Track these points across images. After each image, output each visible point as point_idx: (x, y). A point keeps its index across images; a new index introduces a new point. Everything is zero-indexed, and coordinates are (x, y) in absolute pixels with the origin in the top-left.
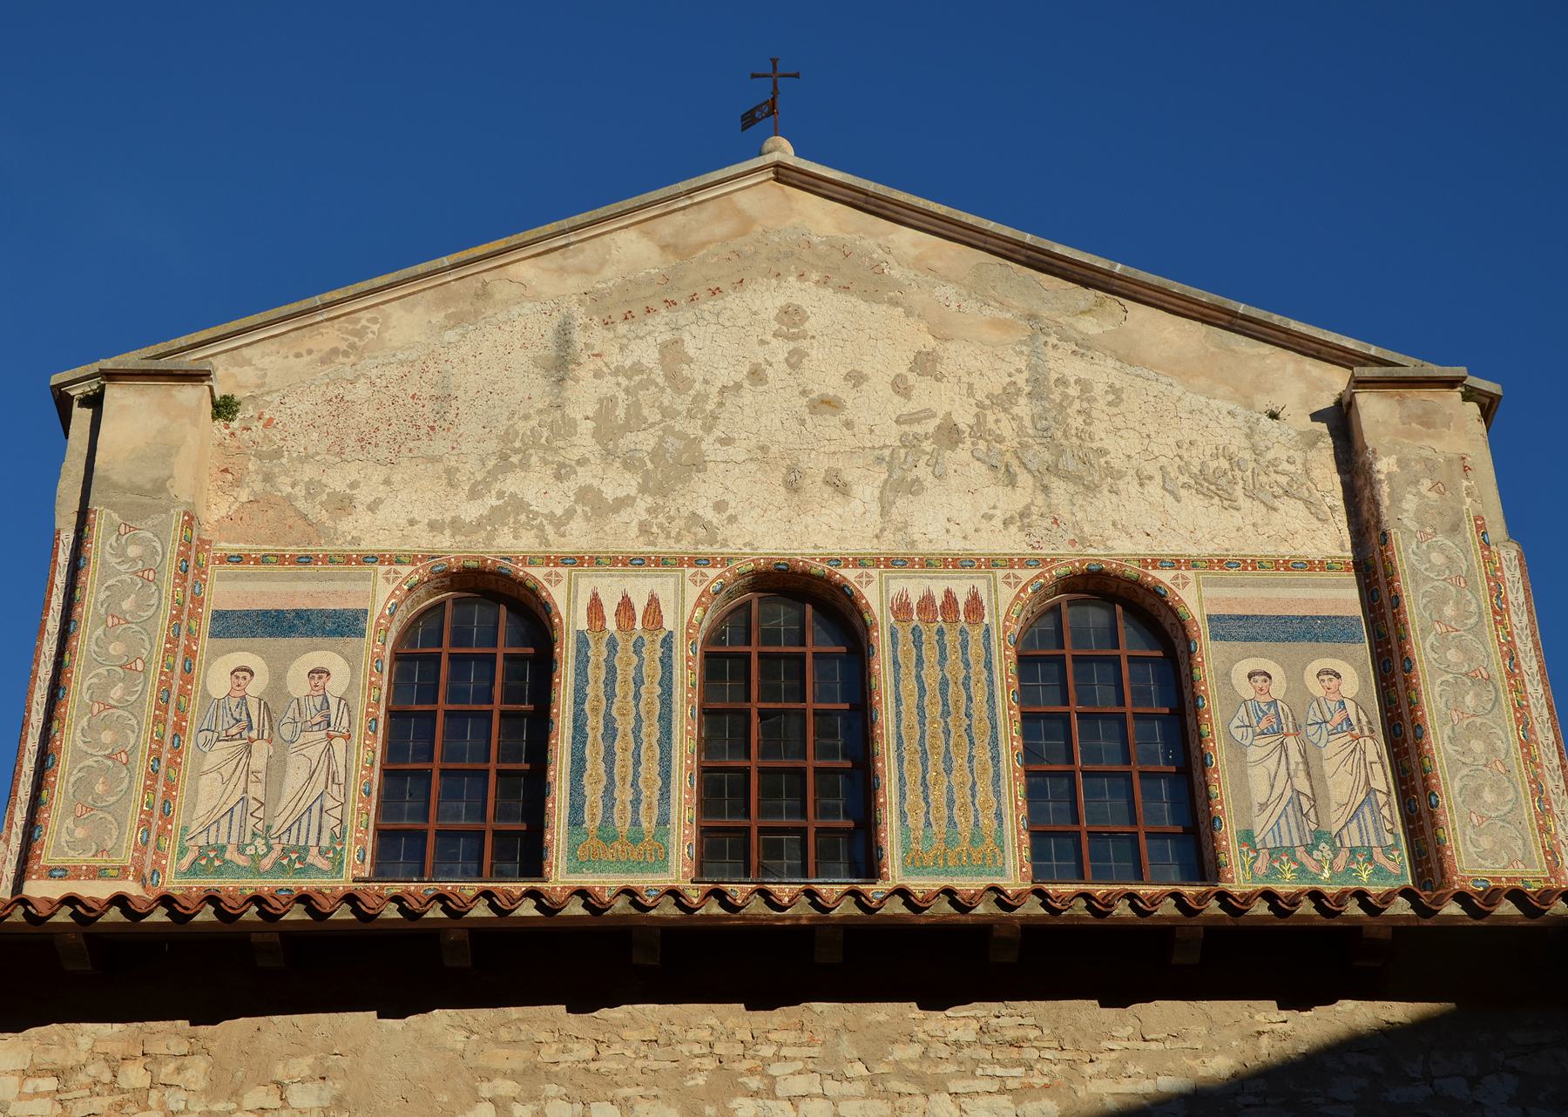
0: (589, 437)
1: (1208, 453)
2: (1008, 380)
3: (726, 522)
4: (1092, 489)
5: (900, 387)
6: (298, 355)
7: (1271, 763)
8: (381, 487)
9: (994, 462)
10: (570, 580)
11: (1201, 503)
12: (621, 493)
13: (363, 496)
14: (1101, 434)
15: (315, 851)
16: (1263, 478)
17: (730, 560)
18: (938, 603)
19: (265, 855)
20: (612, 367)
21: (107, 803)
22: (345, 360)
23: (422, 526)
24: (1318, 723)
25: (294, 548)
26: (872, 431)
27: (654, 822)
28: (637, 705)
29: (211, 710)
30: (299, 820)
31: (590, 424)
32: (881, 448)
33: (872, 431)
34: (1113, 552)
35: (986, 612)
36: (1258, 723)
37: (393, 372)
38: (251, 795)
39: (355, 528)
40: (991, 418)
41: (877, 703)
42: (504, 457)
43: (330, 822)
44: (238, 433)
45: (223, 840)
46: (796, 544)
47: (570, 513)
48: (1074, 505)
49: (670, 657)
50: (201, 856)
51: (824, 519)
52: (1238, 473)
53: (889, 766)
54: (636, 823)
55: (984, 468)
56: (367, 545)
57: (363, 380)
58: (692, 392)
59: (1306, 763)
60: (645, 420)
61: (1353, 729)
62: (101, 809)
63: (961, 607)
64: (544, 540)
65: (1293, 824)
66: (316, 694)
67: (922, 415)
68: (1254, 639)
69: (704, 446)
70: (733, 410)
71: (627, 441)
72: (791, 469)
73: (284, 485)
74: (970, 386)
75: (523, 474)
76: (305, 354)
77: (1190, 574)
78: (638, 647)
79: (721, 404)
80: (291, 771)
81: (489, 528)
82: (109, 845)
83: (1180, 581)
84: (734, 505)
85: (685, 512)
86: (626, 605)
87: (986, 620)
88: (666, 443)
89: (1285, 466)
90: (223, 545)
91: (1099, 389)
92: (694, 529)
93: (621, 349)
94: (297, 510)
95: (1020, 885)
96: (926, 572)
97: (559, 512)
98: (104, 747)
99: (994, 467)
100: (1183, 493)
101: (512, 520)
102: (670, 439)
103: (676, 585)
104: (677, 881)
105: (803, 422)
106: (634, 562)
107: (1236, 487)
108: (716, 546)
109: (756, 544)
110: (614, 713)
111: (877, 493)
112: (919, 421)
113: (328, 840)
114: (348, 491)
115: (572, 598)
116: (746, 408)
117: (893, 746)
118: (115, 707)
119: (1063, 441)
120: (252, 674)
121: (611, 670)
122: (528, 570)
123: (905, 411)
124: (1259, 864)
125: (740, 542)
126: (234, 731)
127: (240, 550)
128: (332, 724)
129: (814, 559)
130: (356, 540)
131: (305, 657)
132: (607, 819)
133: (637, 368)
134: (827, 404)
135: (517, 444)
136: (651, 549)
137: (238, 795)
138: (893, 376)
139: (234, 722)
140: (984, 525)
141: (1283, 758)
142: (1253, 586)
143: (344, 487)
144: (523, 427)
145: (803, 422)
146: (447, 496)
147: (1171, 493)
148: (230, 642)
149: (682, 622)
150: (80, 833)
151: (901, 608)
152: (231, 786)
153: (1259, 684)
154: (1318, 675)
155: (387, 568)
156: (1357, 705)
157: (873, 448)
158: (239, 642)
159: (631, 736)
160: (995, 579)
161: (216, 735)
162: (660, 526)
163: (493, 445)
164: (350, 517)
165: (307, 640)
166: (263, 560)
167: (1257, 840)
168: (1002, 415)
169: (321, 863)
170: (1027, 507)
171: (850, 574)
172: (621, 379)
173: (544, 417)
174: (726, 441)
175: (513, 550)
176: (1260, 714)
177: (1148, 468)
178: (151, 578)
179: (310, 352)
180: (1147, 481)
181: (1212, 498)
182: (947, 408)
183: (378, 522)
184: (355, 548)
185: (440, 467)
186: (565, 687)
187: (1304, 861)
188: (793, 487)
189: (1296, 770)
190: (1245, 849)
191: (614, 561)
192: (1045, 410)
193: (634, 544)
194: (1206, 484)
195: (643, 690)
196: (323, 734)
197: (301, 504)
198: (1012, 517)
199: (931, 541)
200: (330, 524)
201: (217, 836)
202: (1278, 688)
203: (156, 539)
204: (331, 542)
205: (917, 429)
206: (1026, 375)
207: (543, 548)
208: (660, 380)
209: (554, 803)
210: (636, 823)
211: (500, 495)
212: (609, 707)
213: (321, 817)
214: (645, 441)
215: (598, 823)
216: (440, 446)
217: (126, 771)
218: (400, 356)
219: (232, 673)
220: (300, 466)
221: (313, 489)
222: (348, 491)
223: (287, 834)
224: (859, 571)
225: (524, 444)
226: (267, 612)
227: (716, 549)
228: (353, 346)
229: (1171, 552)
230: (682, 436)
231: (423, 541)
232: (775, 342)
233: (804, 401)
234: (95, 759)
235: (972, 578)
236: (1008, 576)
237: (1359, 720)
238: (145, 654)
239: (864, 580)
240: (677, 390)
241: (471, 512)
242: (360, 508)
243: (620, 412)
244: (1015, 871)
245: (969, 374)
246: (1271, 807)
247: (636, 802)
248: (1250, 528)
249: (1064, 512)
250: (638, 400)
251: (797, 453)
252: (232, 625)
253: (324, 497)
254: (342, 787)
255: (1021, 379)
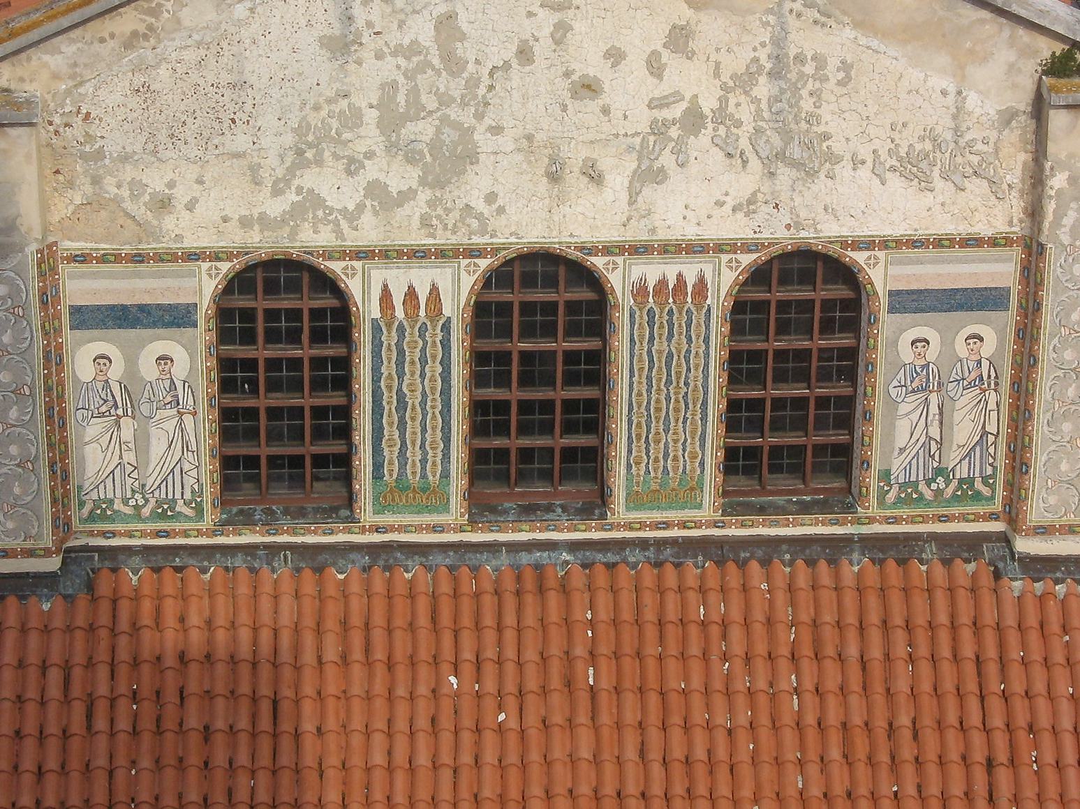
0: (373, 127)
1: (916, 135)
2: (752, 55)
3: (495, 214)
4: (812, 174)
5: (655, 67)
6: (102, 40)
7: (915, 416)
8: (196, 186)
9: (730, 150)
10: (364, 273)
11: (902, 185)
12: (405, 188)
13: (181, 195)
14: (830, 122)
15: (181, 502)
16: (959, 159)
17: (498, 250)
18: (671, 286)
19: (144, 506)
20: (392, 45)
21: (26, 502)
22: (146, 44)
23: (234, 223)
24: (957, 380)
25: (127, 247)
26: (625, 117)
27: (438, 475)
28: (422, 383)
29: (83, 391)
30: (166, 479)
31: (374, 113)
32: (633, 136)
33: (625, 117)
34: (821, 235)
35: (709, 294)
36: (912, 382)
37: (190, 56)
38: (126, 459)
39: (177, 226)
40: (732, 102)
41: (615, 374)
42: (300, 153)
43: (190, 481)
44: (61, 130)
45: (110, 495)
46: (555, 233)
47: (360, 207)
48: (794, 190)
49: (449, 340)
50: (96, 507)
51: (580, 209)
52: (938, 154)
53: (621, 428)
54: (424, 476)
55: (721, 154)
56: (191, 243)
57: (164, 66)
58: (465, 75)
59: (941, 414)
60: (424, 108)
61: (984, 384)
62: (22, 506)
63: (690, 290)
64: (339, 233)
65: (921, 464)
66: (164, 377)
67: (672, 99)
68: (922, 311)
69: (476, 137)
70: (502, 94)
71: (410, 130)
72: (553, 160)
73: (109, 184)
74: (718, 64)
75: (317, 170)
76: (108, 39)
77: (881, 254)
78: (423, 331)
79: (491, 88)
80: (154, 441)
81: (292, 223)
82: (34, 532)
83: (872, 262)
84: (501, 195)
85: (460, 204)
86: (411, 294)
87: (709, 302)
88: (443, 134)
89: (979, 147)
90: (68, 244)
91: (833, 63)
92: (468, 221)
93: (400, 27)
94: (124, 211)
95: (712, 516)
96: (665, 258)
97: (351, 207)
98: (12, 458)
99: (729, 155)
100: (889, 175)
101: (311, 216)
102: (446, 130)
103: (453, 276)
104: (456, 518)
105: (564, 108)
106: (417, 254)
107: (934, 168)
108: (487, 236)
109: (521, 234)
110: (405, 389)
111: (626, 184)
112: (667, 105)
113: (190, 494)
114: (167, 191)
115: (366, 291)
116: (514, 92)
117: (625, 411)
118: (14, 426)
119: (793, 126)
120: (110, 362)
121: (401, 353)
122: (326, 263)
123: (657, 94)
124: (890, 495)
125: (507, 232)
126: (104, 409)
127: (82, 249)
128: (181, 403)
129: (570, 247)
130: (179, 237)
131: (151, 346)
132: (402, 472)
133: (413, 49)
134: (589, 88)
135: (310, 138)
136: (432, 241)
137: (116, 460)
138: (649, 51)
139: (103, 402)
140: (717, 212)
141: (925, 410)
142: (930, 263)
143: (163, 187)
144: (314, 119)
145: (564, 108)
146: (252, 192)
147: (877, 175)
148: (87, 333)
149: (458, 308)
150: (10, 525)
151: (640, 291)
152: (109, 454)
153: (918, 350)
154: (966, 340)
155: (210, 264)
156: (990, 363)
157: (626, 135)
158: (96, 332)
159: (419, 409)
160: (720, 264)
161: (90, 412)
162: (438, 217)
163: (289, 139)
164: (171, 215)
165: (150, 332)
166: (103, 259)
167: (892, 477)
168: (742, 98)
169: (188, 511)
170: (754, 194)
171: (598, 262)
172: (401, 61)
173: (333, 107)
174: (496, 130)
175: (313, 244)
176: (915, 375)
177: (862, 151)
178: (21, 314)
179: (112, 36)
180: (859, 165)
181: (912, 180)
182: (695, 90)
183: (196, 220)
184: (179, 246)
185: (244, 162)
186: (364, 366)
187: (924, 491)
188: (554, 177)
189: (932, 421)
190: (882, 484)
191: (400, 254)
192: (782, 91)
193: (418, 238)
194: (909, 166)
195: (427, 369)
196: (174, 411)
197: (128, 205)
198: (740, 205)
199: (669, 227)
200: (155, 222)
201: (105, 492)
202: (932, 353)
203: (17, 277)
204: (158, 240)
205: (668, 114)
206: (768, 49)
207: (339, 243)
208: (436, 62)
209: (360, 462)
210: (424, 476)
211: (299, 190)
212: (400, 384)
213: (182, 477)
214: (423, 130)
215: (395, 476)
216: (241, 141)
217: (34, 477)
218: (196, 37)
219: (94, 360)
220: (121, 165)
221: (137, 188)
222: (167, 191)
223: (158, 490)
224: (607, 258)
225: (317, 138)
226: (114, 306)
227: (486, 239)
228: (151, 28)
229: (870, 233)
230: (457, 126)
231: (235, 238)
232: (542, 13)
233: (566, 84)
234: (9, 467)
235: (701, 262)
236: (730, 261)
237: (989, 376)
238: (29, 380)
239: (611, 266)
240: (453, 74)
241: (275, 207)
242: (180, 207)
243: (401, 98)
244: (710, 505)
245: (718, 50)
246: (908, 451)
247: (424, 461)
248: (938, 207)
249: (784, 197)
250: (416, 85)
251: (559, 141)
252: (88, 318)
253: (147, 197)
254: (195, 453)
255: (763, 55)
